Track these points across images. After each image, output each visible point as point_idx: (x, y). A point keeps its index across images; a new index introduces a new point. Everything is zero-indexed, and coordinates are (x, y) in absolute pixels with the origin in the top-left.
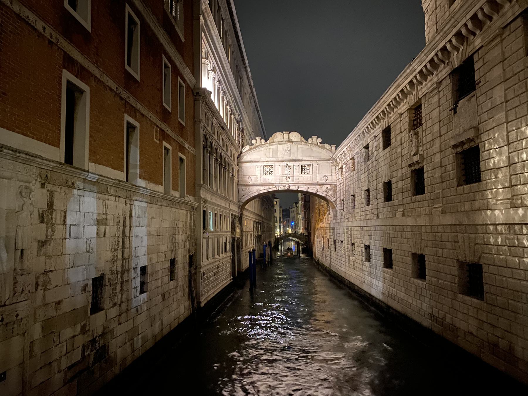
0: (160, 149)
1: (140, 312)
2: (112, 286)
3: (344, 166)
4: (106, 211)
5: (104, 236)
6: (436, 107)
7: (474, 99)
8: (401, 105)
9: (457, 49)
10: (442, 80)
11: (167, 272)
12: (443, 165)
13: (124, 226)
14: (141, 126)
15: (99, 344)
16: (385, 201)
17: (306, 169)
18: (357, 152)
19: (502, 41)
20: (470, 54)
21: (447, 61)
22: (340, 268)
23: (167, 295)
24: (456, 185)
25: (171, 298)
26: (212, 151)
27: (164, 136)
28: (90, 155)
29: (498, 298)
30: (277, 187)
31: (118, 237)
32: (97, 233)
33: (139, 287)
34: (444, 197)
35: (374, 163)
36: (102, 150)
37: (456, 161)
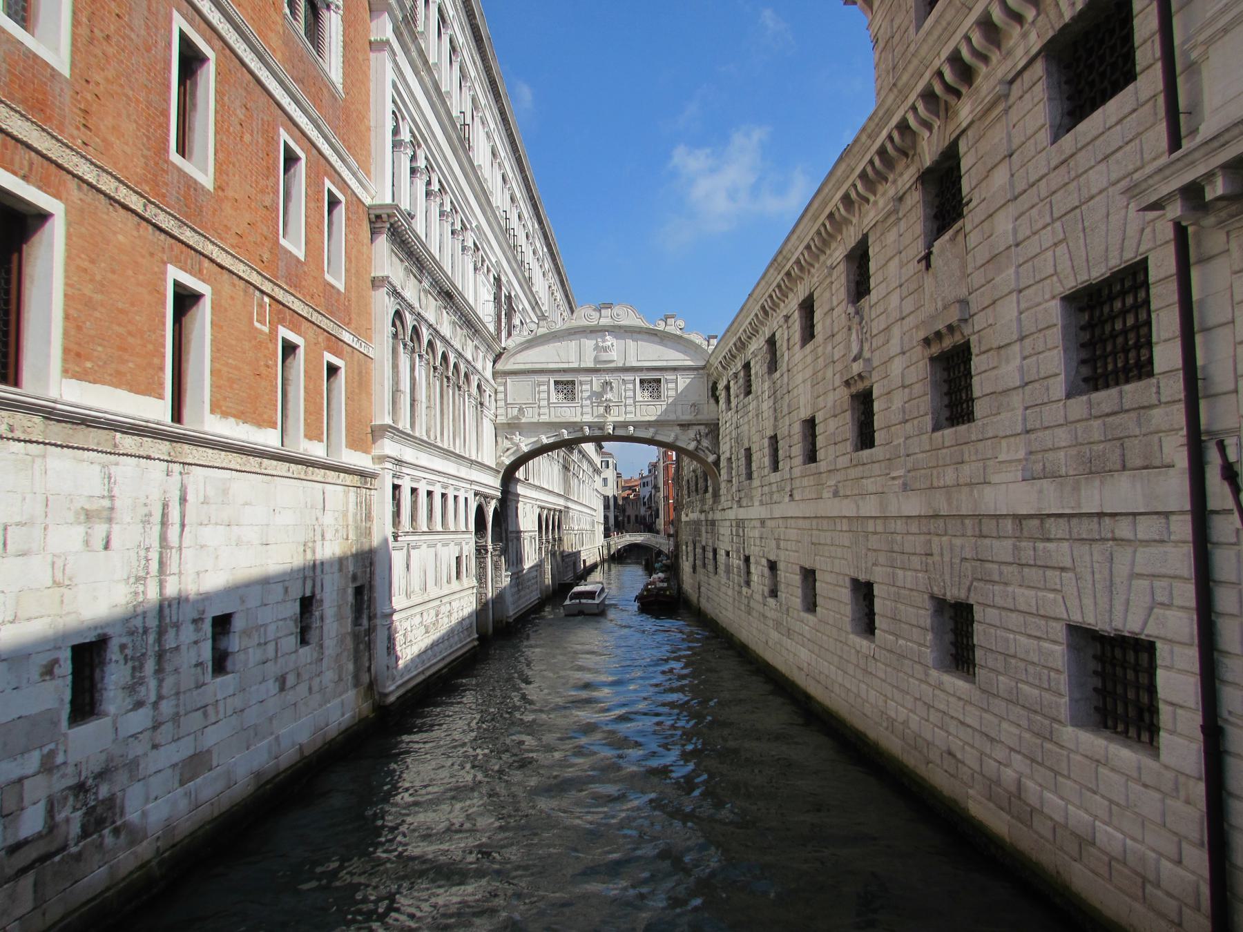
0: (270, 346)
1: (214, 721)
2: (130, 664)
3: (732, 383)
4: (110, 490)
5: (107, 547)
6: (894, 252)
7: (960, 237)
8: (832, 248)
9: (928, 126)
10: (905, 193)
11: (293, 628)
12: (907, 383)
13: (164, 523)
14: (215, 292)
15: (96, 793)
16: (804, 463)
17: (650, 389)
18: (753, 352)
19: (1006, 111)
20: (954, 136)
21: (911, 153)
22: (723, 611)
23: (291, 680)
24: (929, 429)
25: (302, 689)
27: (282, 312)
28: (65, 360)
29: (1001, 678)
31: (147, 549)
32: (87, 543)
33: (210, 664)
34: (908, 456)
35: (785, 376)
36: (100, 349)
37: (931, 374)
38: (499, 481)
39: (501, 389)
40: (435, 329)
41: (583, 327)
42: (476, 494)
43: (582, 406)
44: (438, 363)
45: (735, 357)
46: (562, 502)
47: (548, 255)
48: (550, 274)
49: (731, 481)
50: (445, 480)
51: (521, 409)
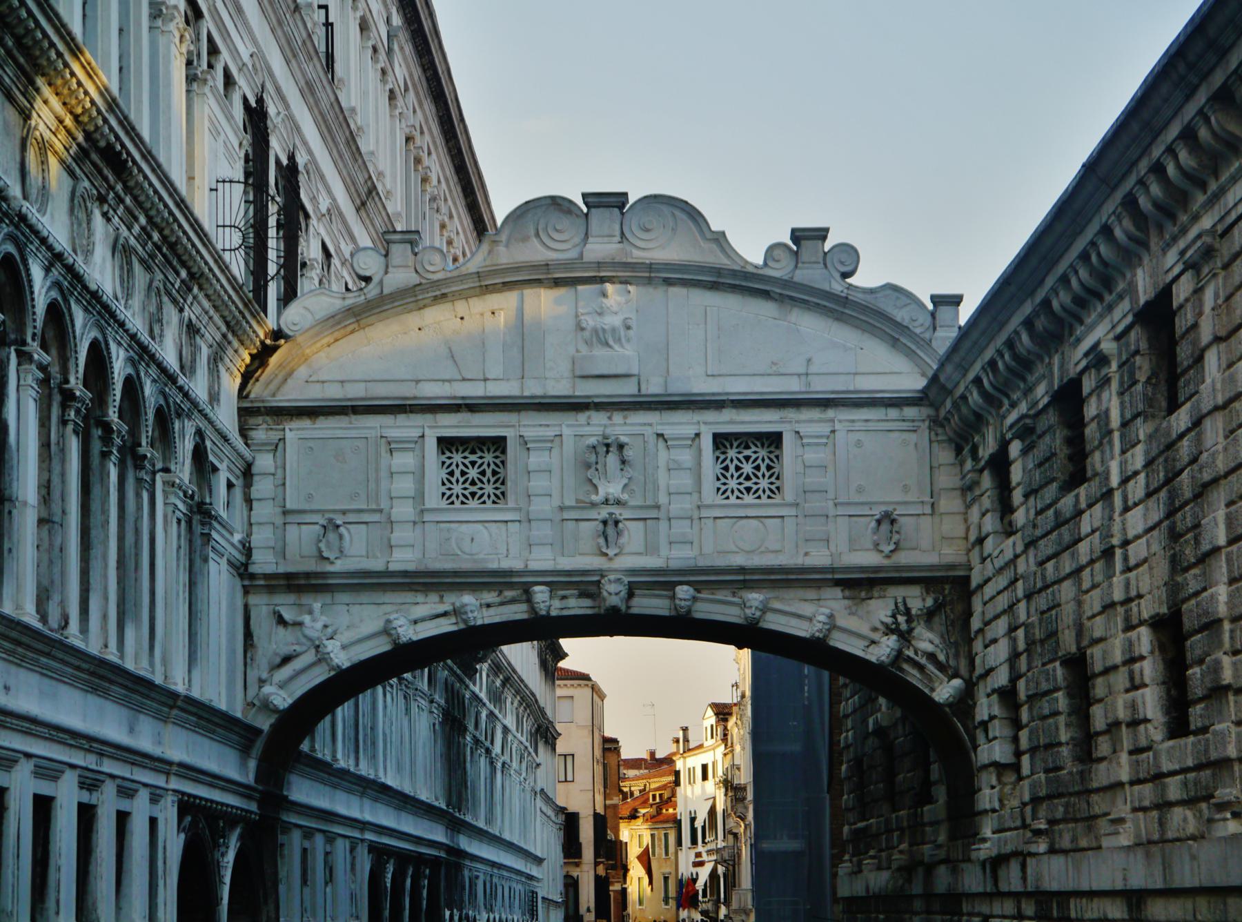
3: (1015, 448)
17: (747, 468)
26: (21, 329)
30: (541, 594)
35: (1214, 430)
38: (252, 764)
39: (264, 462)
40: (70, 269)
41: (534, 267)
42: (187, 805)
43: (530, 521)
44: (75, 382)
45: (1024, 365)
46: (438, 834)
47: (403, 37)
48: (411, 93)
49: (1016, 767)
50: (90, 761)
51: (331, 527)
